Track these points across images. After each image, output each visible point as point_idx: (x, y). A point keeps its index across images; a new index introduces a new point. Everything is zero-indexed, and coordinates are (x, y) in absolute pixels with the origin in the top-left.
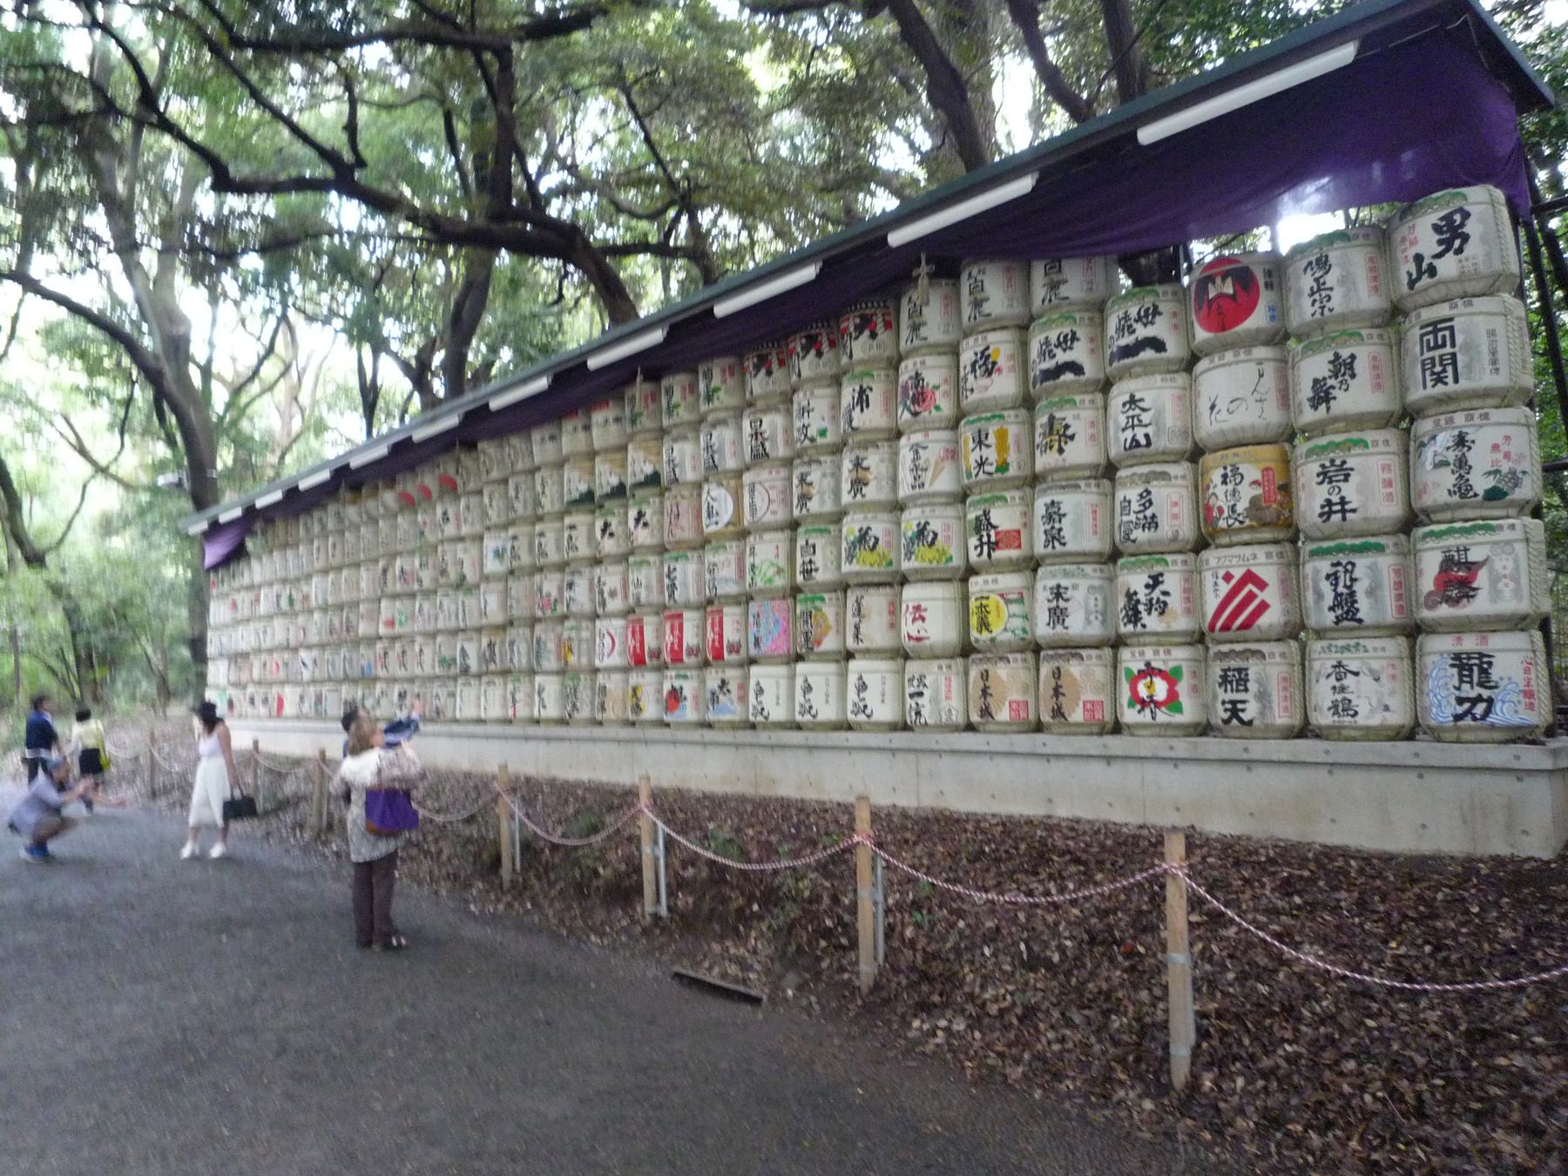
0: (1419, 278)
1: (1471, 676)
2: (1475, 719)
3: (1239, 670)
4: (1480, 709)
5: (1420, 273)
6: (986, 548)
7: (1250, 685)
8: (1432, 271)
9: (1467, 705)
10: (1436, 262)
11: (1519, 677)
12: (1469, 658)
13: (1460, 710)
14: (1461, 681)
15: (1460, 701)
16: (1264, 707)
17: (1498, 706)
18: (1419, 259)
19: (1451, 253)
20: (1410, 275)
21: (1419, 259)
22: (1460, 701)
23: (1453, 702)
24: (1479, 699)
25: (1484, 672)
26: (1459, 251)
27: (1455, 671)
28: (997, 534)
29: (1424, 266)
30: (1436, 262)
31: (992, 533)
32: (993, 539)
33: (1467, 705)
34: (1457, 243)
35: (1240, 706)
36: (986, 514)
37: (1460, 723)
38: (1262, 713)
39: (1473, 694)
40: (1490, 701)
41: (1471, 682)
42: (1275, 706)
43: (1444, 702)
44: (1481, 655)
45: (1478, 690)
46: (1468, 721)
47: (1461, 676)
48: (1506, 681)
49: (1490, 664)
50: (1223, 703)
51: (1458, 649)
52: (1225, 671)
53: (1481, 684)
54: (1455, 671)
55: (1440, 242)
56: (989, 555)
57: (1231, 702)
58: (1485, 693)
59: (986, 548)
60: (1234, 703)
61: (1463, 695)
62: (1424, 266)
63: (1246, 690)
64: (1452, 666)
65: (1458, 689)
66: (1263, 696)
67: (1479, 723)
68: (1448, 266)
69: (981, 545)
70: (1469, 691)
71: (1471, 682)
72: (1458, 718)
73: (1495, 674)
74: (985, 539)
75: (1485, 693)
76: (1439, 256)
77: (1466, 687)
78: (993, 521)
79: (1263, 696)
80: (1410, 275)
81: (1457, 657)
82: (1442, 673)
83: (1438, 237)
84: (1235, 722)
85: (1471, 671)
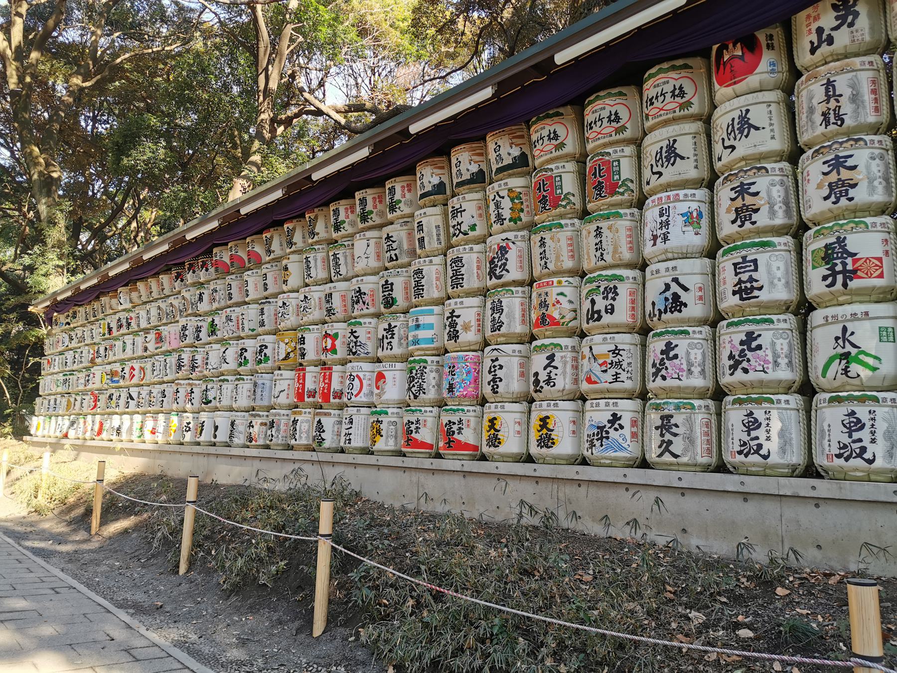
0: (819, 46)
5: (820, 42)
6: (840, 278)
8: (830, 41)
10: (833, 33)
18: (820, 31)
19: (845, 26)
20: (812, 43)
21: (820, 31)
26: (851, 25)
28: (855, 262)
29: (824, 37)
30: (833, 33)
31: (849, 261)
32: (850, 267)
34: (850, 18)
36: (841, 241)
55: (837, 18)
56: (845, 285)
59: (840, 278)
62: (824, 37)
68: (842, 38)
69: (834, 274)
74: (839, 268)
76: (833, 29)
78: (851, 248)
80: (812, 43)
83: (836, 14)
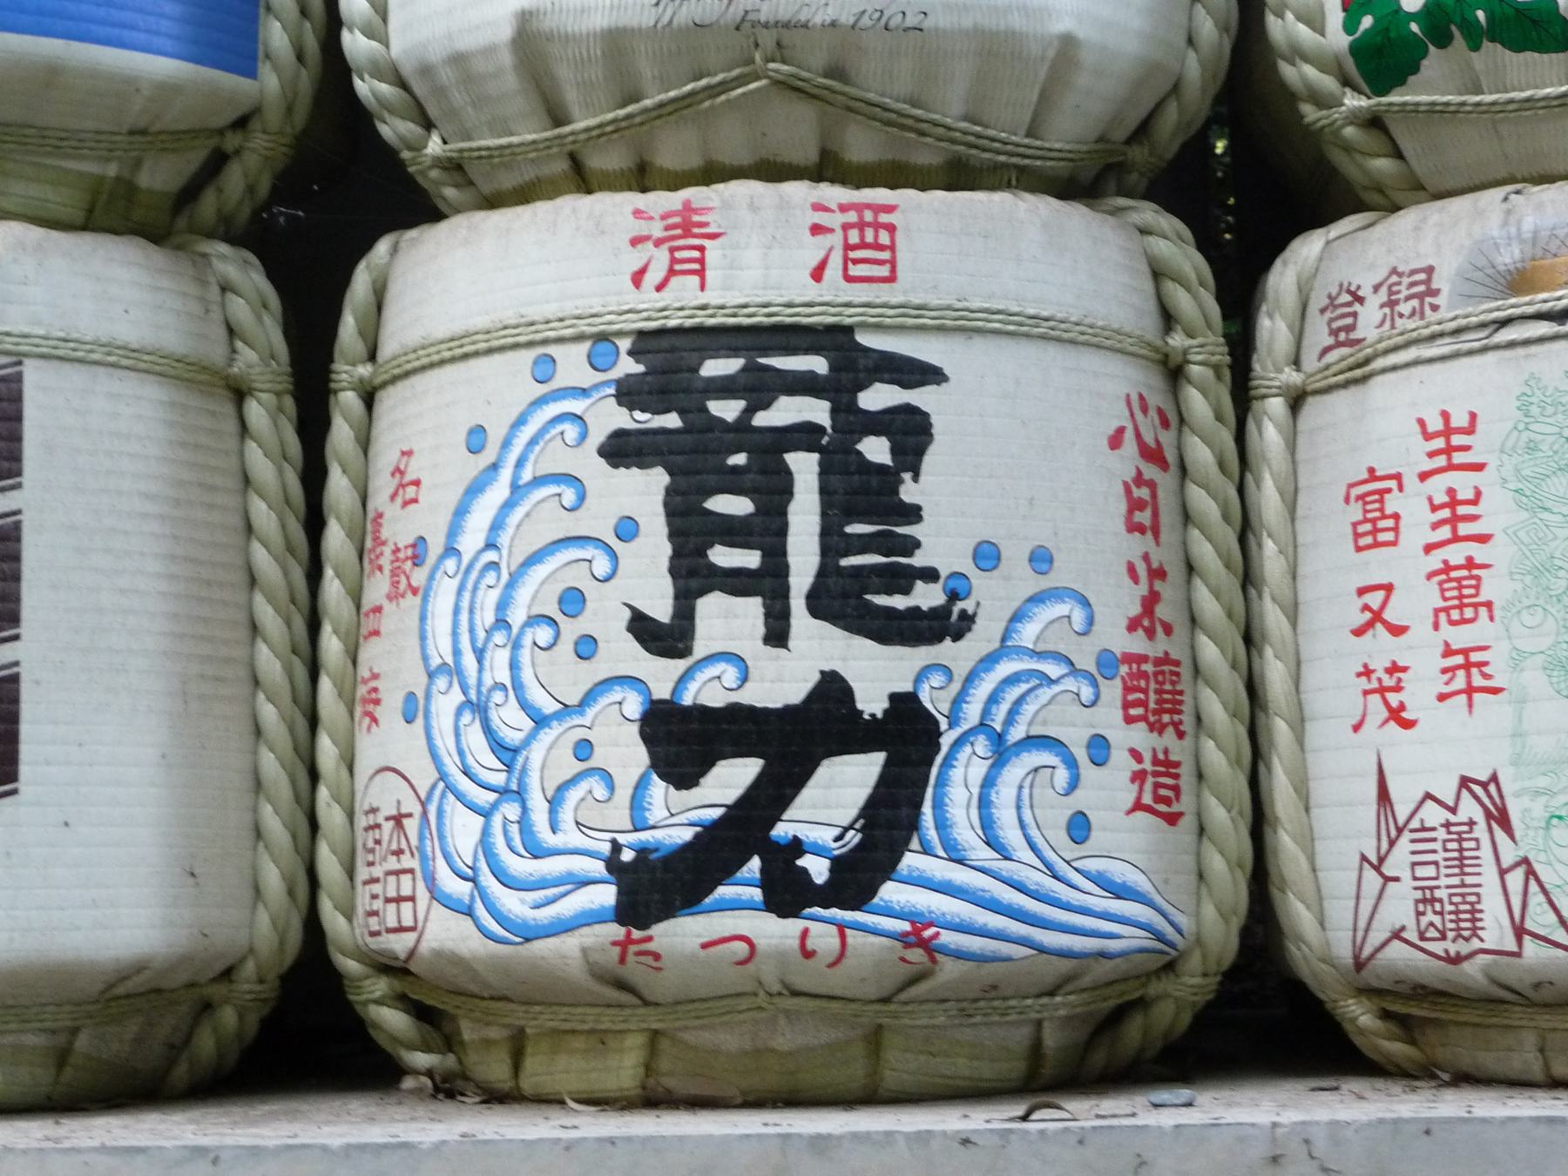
1: (767, 530)
2: (787, 892)
4: (837, 793)
9: (732, 778)
12: (760, 388)
13: (677, 816)
14: (693, 576)
15: (681, 740)
17: (960, 777)
23: (627, 754)
24: (827, 721)
25: (869, 499)
27: (645, 491)
33: (732, 778)
37: (681, 934)
39: (781, 682)
40: (908, 735)
41: (768, 584)
43: (548, 758)
44: (849, 361)
45: (819, 647)
46: (734, 920)
47: (691, 532)
49: (911, 433)
51: (682, 303)
53: (840, 600)
54: (645, 491)
61: (710, 689)
64: (622, 450)
65: (664, 638)
67: (820, 928)
70: (751, 661)
71: (768, 584)
72: (656, 885)
73: (950, 508)
75: (876, 674)
77: (727, 621)
81: (666, 363)
82: (544, 517)
85: (774, 492)
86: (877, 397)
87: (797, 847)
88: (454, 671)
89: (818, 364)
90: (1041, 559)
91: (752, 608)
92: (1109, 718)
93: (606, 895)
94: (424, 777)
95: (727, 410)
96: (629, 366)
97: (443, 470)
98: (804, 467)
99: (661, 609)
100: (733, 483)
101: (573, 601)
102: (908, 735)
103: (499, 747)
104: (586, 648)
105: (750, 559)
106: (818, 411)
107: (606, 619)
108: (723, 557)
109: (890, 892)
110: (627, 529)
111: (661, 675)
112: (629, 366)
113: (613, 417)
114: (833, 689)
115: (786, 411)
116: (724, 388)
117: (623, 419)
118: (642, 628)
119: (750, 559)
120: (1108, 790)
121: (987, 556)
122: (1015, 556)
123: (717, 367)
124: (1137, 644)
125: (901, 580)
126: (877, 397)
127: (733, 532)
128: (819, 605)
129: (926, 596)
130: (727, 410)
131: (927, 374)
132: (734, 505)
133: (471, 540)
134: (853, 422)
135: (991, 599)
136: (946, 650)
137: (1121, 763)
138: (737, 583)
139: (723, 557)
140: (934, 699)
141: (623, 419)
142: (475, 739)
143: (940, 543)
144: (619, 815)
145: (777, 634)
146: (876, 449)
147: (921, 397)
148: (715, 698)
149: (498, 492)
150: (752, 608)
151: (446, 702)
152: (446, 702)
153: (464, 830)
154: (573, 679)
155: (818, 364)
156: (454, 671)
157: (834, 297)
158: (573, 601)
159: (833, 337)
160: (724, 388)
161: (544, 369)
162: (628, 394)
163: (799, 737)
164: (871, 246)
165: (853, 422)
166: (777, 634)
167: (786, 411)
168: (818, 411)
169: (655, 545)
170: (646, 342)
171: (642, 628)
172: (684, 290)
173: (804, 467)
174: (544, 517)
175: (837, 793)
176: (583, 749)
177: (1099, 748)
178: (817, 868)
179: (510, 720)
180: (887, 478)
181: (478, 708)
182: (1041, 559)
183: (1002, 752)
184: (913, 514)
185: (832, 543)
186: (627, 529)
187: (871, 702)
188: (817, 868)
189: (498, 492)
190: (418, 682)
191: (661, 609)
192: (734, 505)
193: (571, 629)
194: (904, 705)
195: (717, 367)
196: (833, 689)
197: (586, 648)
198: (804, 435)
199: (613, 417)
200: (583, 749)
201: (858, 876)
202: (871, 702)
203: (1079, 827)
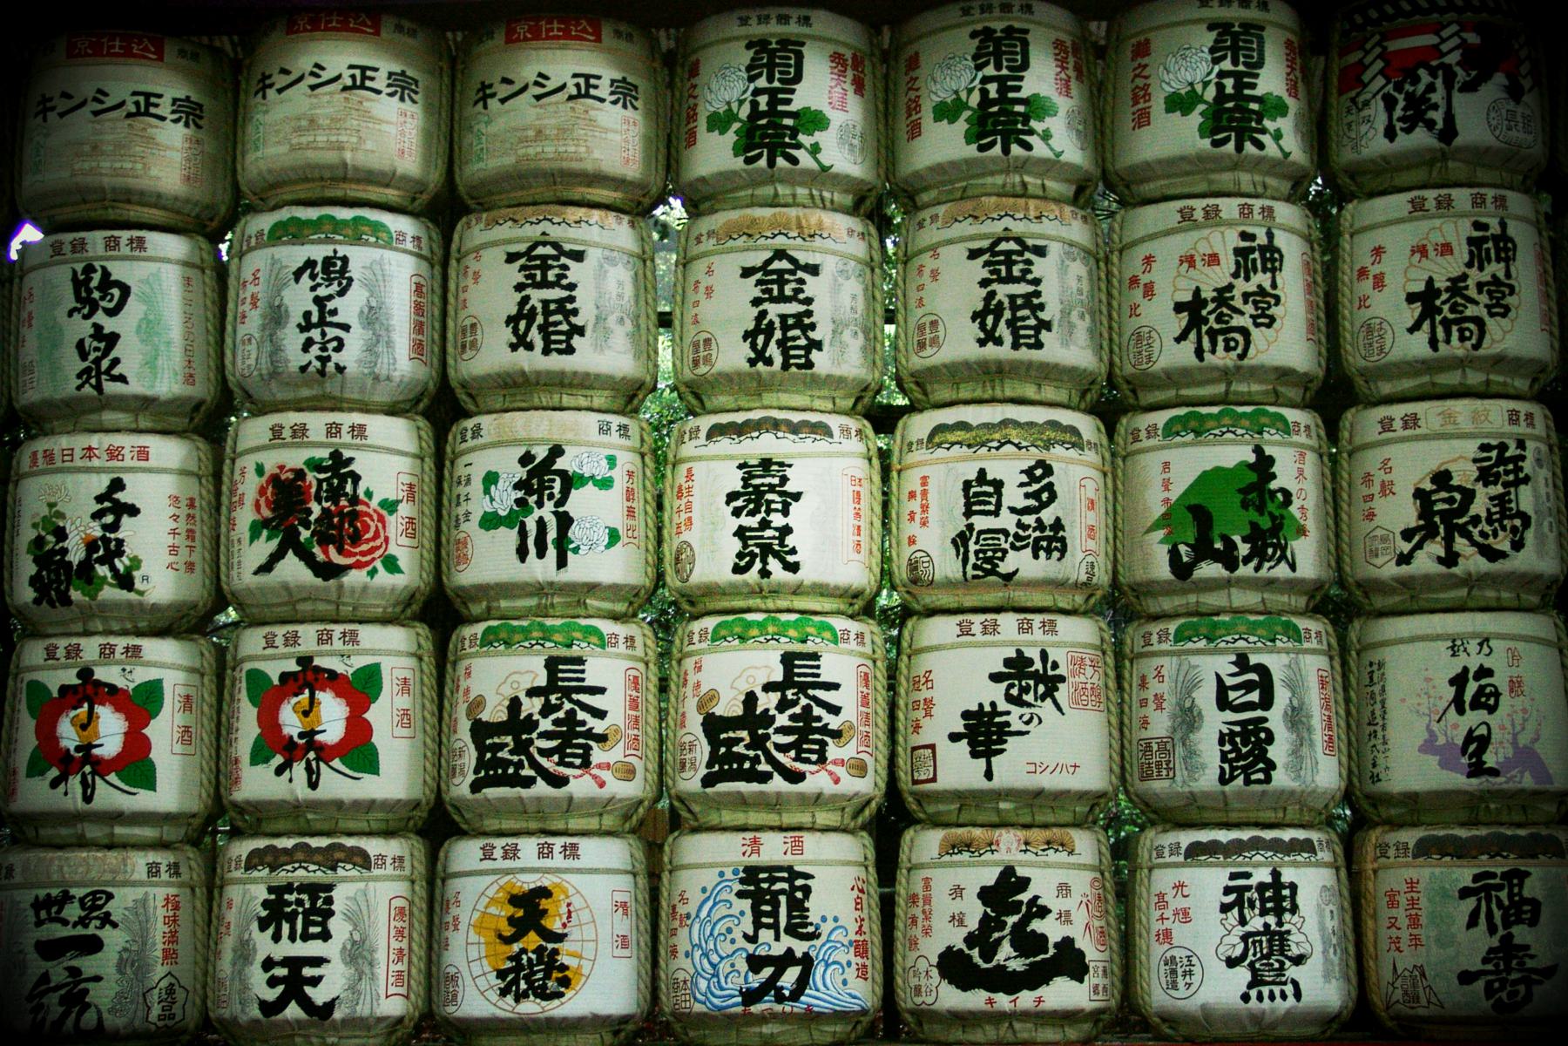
1: (775, 914)
2: (780, 998)
3: (313, 889)
4: (790, 976)
7: (334, 924)
9: (767, 972)
11: (849, 918)
12: (773, 880)
13: (755, 981)
14: (758, 925)
15: (755, 963)
16: (361, 975)
22: (755, 963)
23: (743, 966)
24: (788, 958)
25: (797, 906)
27: (746, 904)
33: (767, 972)
35: (308, 972)
37: (756, 1009)
38: (353, 988)
39: (778, 949)
40: (807, 962)
42: (381, 971)
43: (724, 967)
44: (794, 875)
45: (787, 941)
46: (766, 1005)
47: (757, 914)
48: (830, 924)
49: (807, 890)
50: (268, 964)
51: (754, 860)
52: (279, 890)
53: (792, 931)
54: (746, 904)
57: (287, 962)
58: (800, 948)
60: (294, 963)
61: (762, 951)
63: (325, 936)
64: (740, 895)
65: (752, 939)
66: (357, 953)
72: (750, 997)
73: (816, 908)
75: (800, 948)
77: (766, 935)
79: (357, 953)
81: (751, 874)
84: (293, 1011)
85: (776, 905)
86: (799, 882)
87: (782, 988)
88: (700, 946)
89: (786, 875)
90: (836, 919)
91: (771, 932)
92: (851, 956)
93: (739, 999)
94: (692, 971)
95: (765, 886)
96: (742, 875)
97: (695, 897)
98: (783, 899)
99: (750, 932)
100: (767, 903)
101: (729, 930)
102: (807, 962)
103: (710, 963)
104: (733, 941)
105: (771, 921)
106: (785, 886)
107: (737, 934)
108: (764, 920)
109: (803, 998)
110: (742, 913)
111: (751, 948)
112: (742, 875)
113: (738, 887)
114: (790, 951)
115: (778, 886)
116: (764, 880)
117: (741, 887)
118: (746, 936)
119: (771, 921)
120: (851, 974)
121: (824, 919)
122: (830, 919)
123: (762, 876)
124: (858, 937)
125: (806, 925)
126: (799, 882)
127: (767, 914)
128: (787, 931)
129: (811, 929)
130: (765, 886)
131: (808, 876)
132: (767, 908)
133: (703, 914)
134: (794, 889)
135: (825, 929)
136: (815, 942)
137: (854, 966)
138: (768, 926)
139: (764, 920)
140: (813, 954)
141: (741, 887)
142: (705, 961)
143: (813, 917)
144: (741, 980)
145: (777, 938)
146: (799, 895)
147: (809, 882)
148: (763, 953)
149: (710, 903)
150: (771, 932)
151: (698, 953)
152: (698, 953)
153: (703, 984)
154: (730, 948)
155: (786, 875)
156: (700, 946)
157: (788, 859)
158: (729, 930)
159: (790, 869)
160: (764, 880)
161: (721, 874)
162: (742, 881)
163: (783, 962)
164: (798, 846)
165: (794, 889)
166: (777, 938)
167: (778, 886)
168: (785, 886)
169: (749, 918)
170: (747, 869)
171: (746, 936)
172: (754, 857)
173: (783, 899)
174: (721, 910)
175: (790, 976)
176: (733, 965)
177: (849, 964)
178: (787, 993)
179: (715, 958)
180: (802, 902)
181: (706, 955)
182: (836, 919)
183: (827, 965)
184: (807, 910)
185: (790, 917)
186: (742, 913)
187: (799, 954)
188: (787, 993)
189: (710, 903)
190: (689, 948)
191: (750, 932)
192: (767, 908)
193: (729, 937)
194: (806, 955)
195: (762, 876)
196: (790, 951)
197: (733, 941)
198: (782, 892)
199: (738, 887)
200: (733, 965)
201: (797, 994)
202: (799, 954)
203: (845, 982)
